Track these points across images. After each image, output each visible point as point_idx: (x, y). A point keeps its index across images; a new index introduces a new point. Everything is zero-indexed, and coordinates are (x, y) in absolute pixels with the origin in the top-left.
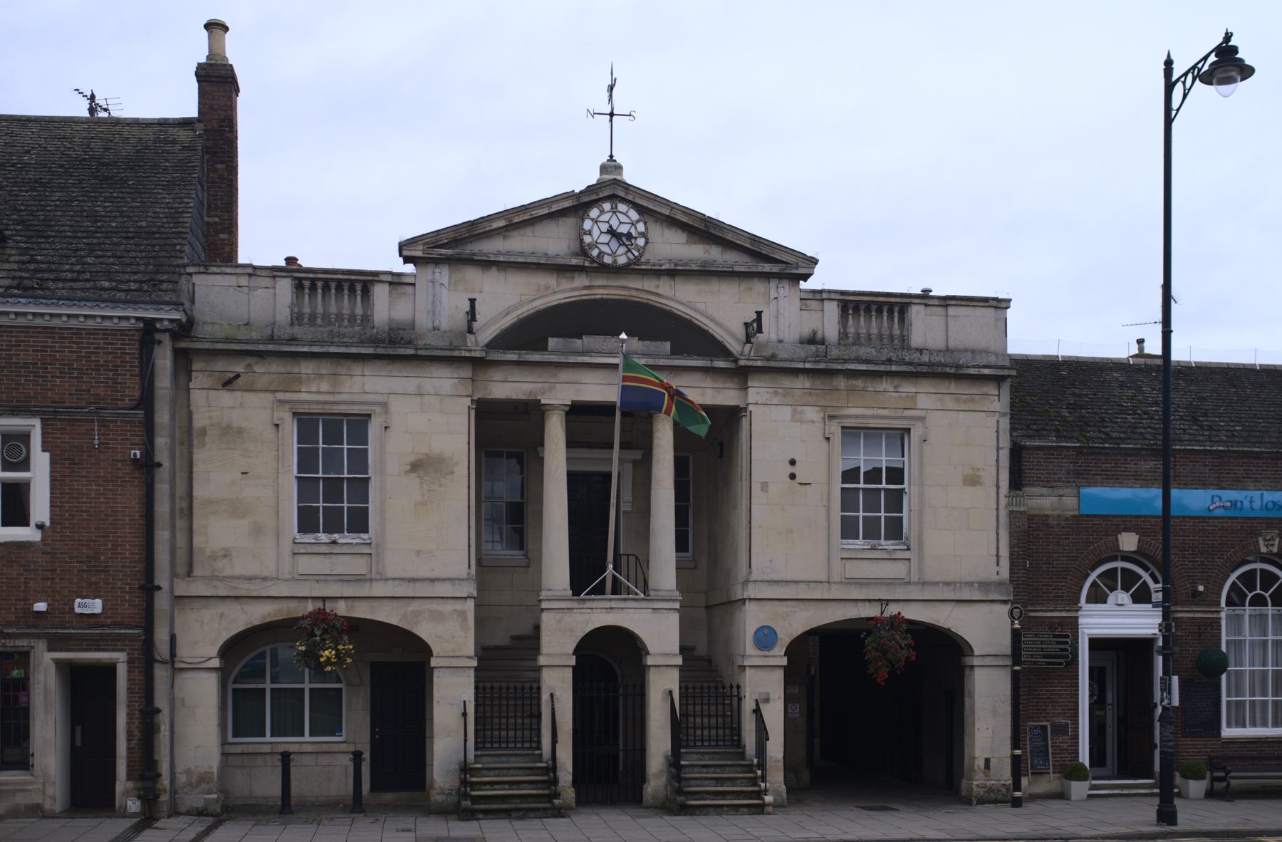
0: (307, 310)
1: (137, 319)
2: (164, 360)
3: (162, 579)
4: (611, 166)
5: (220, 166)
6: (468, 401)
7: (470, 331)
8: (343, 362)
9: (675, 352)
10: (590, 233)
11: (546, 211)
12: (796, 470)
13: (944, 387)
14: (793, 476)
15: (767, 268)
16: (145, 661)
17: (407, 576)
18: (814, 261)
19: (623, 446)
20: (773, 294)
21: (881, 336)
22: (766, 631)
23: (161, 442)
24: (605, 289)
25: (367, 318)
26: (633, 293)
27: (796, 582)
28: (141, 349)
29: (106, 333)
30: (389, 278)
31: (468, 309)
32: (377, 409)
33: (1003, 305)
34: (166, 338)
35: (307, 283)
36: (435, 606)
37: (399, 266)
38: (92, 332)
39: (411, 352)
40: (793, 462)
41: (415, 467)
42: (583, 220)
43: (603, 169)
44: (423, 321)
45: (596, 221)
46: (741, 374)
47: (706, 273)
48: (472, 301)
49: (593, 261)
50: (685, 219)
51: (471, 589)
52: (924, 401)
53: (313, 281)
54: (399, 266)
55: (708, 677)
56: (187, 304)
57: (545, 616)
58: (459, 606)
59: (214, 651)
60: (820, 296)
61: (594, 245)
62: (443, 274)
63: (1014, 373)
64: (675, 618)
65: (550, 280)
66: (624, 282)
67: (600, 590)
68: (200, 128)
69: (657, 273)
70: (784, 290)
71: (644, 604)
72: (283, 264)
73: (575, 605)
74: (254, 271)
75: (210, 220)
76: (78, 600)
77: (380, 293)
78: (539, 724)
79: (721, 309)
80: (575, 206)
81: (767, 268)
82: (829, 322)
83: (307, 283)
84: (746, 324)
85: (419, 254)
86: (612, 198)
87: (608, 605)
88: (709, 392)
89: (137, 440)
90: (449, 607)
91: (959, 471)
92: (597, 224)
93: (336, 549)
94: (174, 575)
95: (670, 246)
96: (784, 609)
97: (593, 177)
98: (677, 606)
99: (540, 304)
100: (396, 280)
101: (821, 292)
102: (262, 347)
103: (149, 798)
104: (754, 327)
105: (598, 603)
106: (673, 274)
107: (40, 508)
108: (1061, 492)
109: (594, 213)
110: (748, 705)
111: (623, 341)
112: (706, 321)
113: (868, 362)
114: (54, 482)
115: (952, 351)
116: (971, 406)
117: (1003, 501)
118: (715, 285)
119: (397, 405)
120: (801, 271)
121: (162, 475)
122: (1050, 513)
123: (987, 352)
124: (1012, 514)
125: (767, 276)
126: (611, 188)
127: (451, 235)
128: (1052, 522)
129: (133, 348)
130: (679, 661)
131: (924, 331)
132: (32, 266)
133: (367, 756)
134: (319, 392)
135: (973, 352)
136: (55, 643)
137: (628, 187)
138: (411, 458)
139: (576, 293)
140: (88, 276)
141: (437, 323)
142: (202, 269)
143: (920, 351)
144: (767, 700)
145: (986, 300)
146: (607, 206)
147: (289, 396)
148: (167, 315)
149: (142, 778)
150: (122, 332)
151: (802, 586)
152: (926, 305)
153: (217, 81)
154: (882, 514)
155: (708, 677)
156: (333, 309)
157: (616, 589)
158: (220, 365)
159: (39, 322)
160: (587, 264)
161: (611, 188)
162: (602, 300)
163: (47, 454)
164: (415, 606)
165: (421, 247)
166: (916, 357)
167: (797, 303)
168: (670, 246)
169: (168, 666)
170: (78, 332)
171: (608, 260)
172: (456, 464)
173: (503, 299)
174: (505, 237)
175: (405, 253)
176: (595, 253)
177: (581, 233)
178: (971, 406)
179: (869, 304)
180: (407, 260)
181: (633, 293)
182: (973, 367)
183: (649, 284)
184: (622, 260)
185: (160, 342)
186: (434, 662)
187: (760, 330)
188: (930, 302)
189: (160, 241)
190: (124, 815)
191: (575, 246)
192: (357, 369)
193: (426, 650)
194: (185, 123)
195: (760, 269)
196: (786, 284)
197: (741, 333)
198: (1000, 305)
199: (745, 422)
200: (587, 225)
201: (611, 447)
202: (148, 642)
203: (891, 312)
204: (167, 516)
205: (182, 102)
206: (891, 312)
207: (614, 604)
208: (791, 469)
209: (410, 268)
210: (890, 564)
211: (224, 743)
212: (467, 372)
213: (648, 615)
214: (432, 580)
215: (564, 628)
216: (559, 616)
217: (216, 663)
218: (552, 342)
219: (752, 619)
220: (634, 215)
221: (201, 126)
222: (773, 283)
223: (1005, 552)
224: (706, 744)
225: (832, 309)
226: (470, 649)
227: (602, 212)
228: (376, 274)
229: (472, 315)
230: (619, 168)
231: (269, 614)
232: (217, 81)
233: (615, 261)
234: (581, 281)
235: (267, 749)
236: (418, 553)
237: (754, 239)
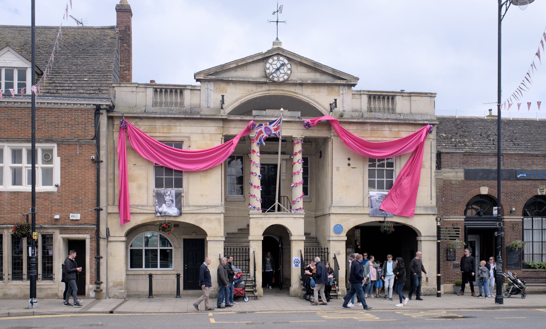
1: (93, 105)
2: (103, 120)
3: (103, 205)
4: (277, 41)
5: (125, 45)
6: (221, 136)
7: (222, 108)
8: (172, 120)
9: (303, 115)
10: (269, 69)
11: (251, 60)
15: (339, 82)
16: (97, 238)
18: (357, 79)
19: (283, 153)
20: (341, 92)
21: (384, 109)
23: (103, 152)
24: (275, 91)
25: (182, 104)
26: (286, 92)
27: (351, 207)
28: (95, 116)
29: (82, 110)
30: (190, 88)
31: (221, 99)
32: (186, 139)
33: (433, 95)
34: (104, 112)
35: (158, 90)
36: (208, 216)
37: (194, 83)
38: (77, 110)
39: (199, 116)
42: (266, 64)
43: (274, 44)
44: (204, 104)
47: (315, 84)
48: (223, 96)
50: (306, 63)
51: (222, 210)
53: (161, 89)
54: (194, 83)
55: (315, 245)
56: (113, 99)
57: (251, 220)
58: (217, 216)
59: (123, 234)
60: (360, 93)
62: (211, 86)
63: (438, 123)
64: (303, 220)
65: (253, 88)
66: (282, 88)
67: (273, 209)
68: (117, 30)
69: (295, 84)
70: (344, 91)
71: (291, 216)
72: (149, 82)
73: (262, 216)
74: (138, 86)
75: (121, 66)
76: (71, 214)
77: (187, 93)
78: (249, 263)
79: (321, 99)
80: (264, 58)
81: (339, 82)
82: (363, 103)
83: (158, 90)
84: (331, 104)
85: (202, 78)
86: (278, 54)
87: (276, 216)
89: (94, 152)
90: (214, 217)
92: (273, 64)
94: (108, 205)
96: (346, 218)
97: (270, 47)
98: (303, 216)
100: (193, 88)
101: (360, 91)
102: (141, 115)
103: (98, 291)
104: (333, 106)
105: (272, 215)
106: (301, 84)
107: (57, 179)
108: (456, 170)
109: (270, 61)
110: (331, 256)
111: (282, 112)
112: (315, 103)
113: (379, 119)
114: (62, 168)
115: (413, 114)
117: (433, 174)
118: (318, 89)
119: (194, 138)
120: (352, 83)
121: (103, 166)
122: (452, 179)
123: (427, 114)
124: (437, 179)
125: (339, 85)
126: (277, 52)
127: (214, 70)
128: (453, 182)
130: (304, 238)
132: (54, 85)
133: (182, 276)
134: (163, 133)
136: (63, 230)
137: (283, 50)
140: (75, 88)
141: (209, 105)
142: (118, 85)
143: (400, 114)
144: (339, 254)
145: (427, 94)
146: (275, 58)
148: (104, 103)
149: (96, 283)
150: (88, 110)
152: (402, 96)
153: (124, 11)
154: (385, 179)
155: (315, 245)
156: (169, 100)
157: (279, 209)
160: (268, 81)
161: (277, 52)
163: (59, 158)
164: (200, 216)
165: (203, 75)
166: (398, 117)
167: (351, 96)
168: (300, 74)
169: (106, 240)
170: (71, 110)
171: (276, 79)
173: (236, 96)
174: (235, 71)
175: (197, 78)
176: (271, 77)
177: (265, 69)
179: (379, 96)
180: (198, 80)
181: (286, 92)
182: (421, 120)
183: (292, 89)
185: (102, 114)
186: (208, 239)
187: (336, 106)
188: (404, 95)
189: (103, 74)
190: (89, 298)
191: (263, 74)
192: (178, 123)
193: (205, 234)
194: (112, 28)
195: (336, 82)
196: (346, 88)
197: (328, 107)
198: (432, 95)
199: (330, 143)
200: (268, 65)
201: (277, 153)
202: (98, 231)
203: (388, 98)
204: (105, 182)
205: (111, 20)
206: (388, 98)
207: (278, 216)
209: (199, 83)
211: (127, 270)
212: (221, 124)
213: (291, 220)
215: (259, 224)
217: (124, 239)
218: (254, 112)
219: (333, 221)
221: (118, 29)
222: (341, 88)
223: (434, 195)
225: (365, 98)
226: (222, 234)
227: (274, 60)
228: (185, 86)
229: (223, 102)
230: (280, 43)
231: (144, 220)
232: (124, 11)
235: (143, 273)
236: (202, 195)
237: (333, 70)
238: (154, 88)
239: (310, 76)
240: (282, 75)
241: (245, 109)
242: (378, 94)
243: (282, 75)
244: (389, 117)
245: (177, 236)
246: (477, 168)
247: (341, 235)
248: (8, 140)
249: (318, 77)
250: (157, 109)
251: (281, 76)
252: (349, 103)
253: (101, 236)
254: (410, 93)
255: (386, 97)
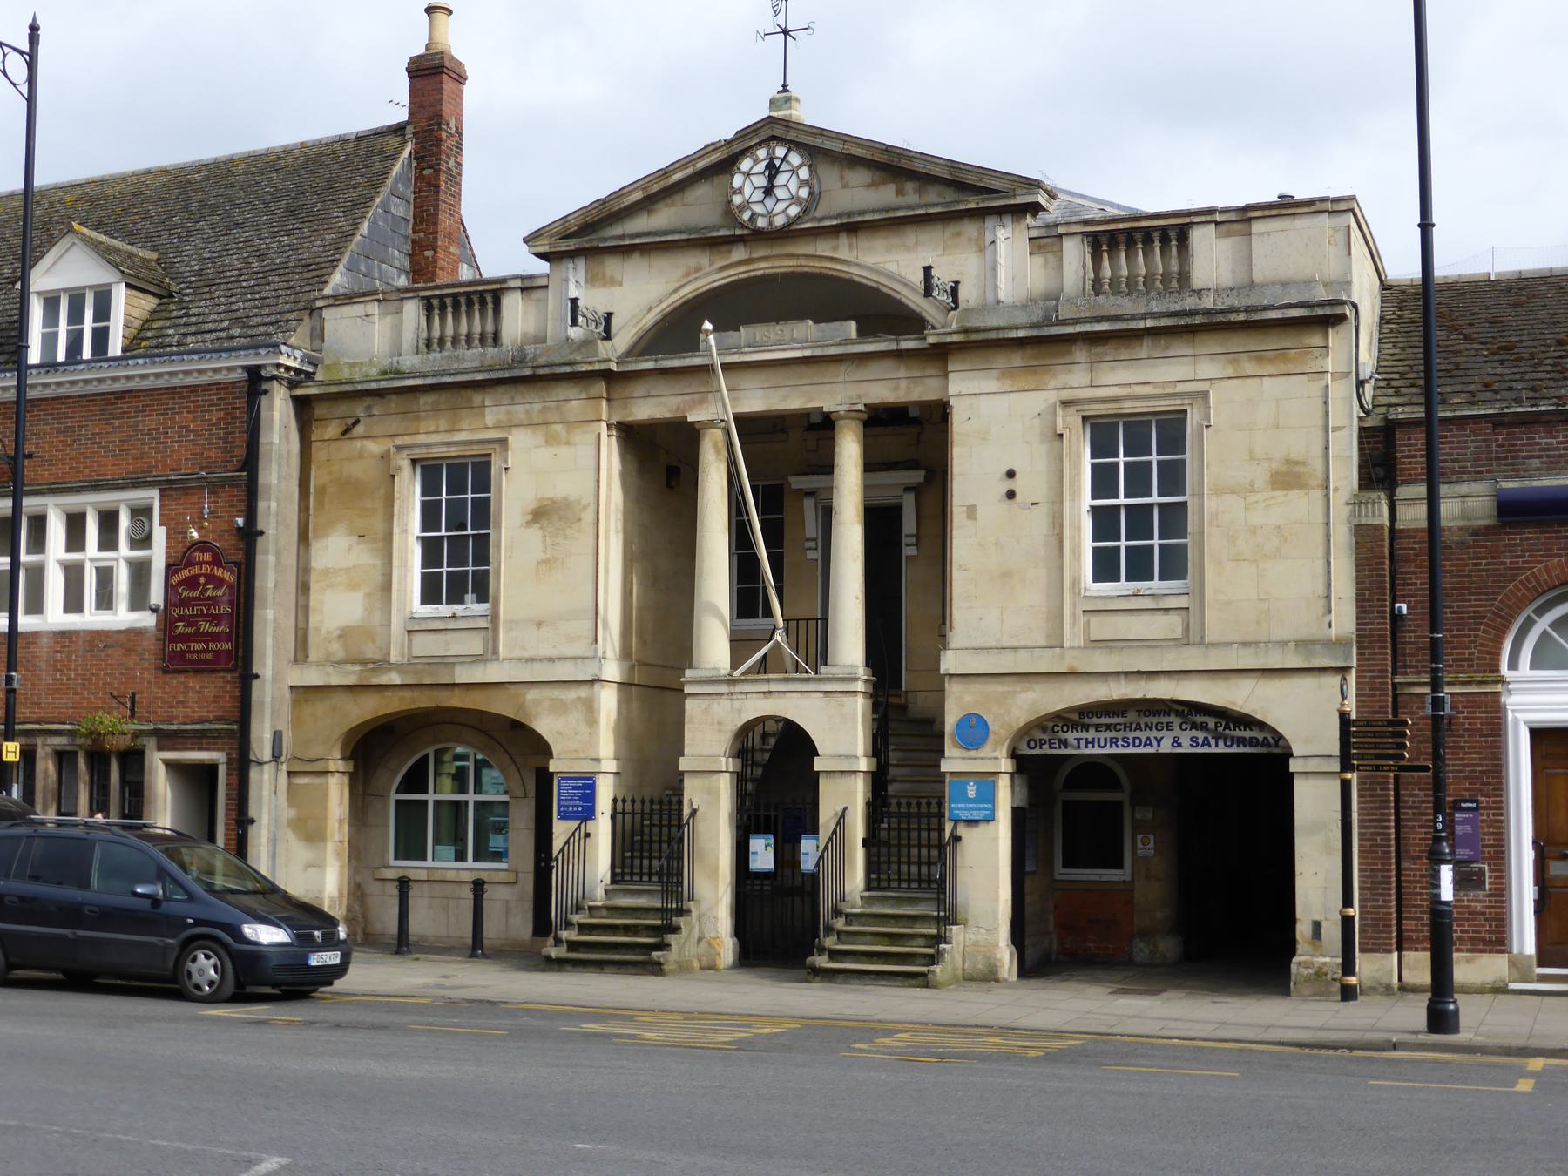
0: (436, 334)
2: (278, 409)
8: (463, 392)
9: (863, 333)
10: (740, 191)
11: (689, 171)
12: (1017, 484)
13: (1238, 342)
14: (1011, 495)
16: (242, 763)
17: (527, 655)
20: (989, 237)
22: (974, 721)
27: (1015, 648)
30: (518, 283)
32: (497, 446)
36: (556, 693)
39: (527, 372)
40: (1011, 474)
41: (541, 514)
42: (732, 176)
45: (748, 175)
46: (940, 354)
49: (743, 226)
52: (1208, 369)
57: (689, 704)
61: (746, 205)
65: (701, 259)
69: (834, 231)
83: (435, 302)
86: (773, 138)
87: (765, 688)
88: (903, 384)
90: (572, 694)
91: (1278, 467)
93: (452, 624)
95: (856, 194)
99: (688, 291)
100: (527, 284)
102: (374, 386)
108: (1464, 489)
116: (1283, 368)
119: (519, 440)
123: (1309, 283)
125: (979, 214)
129: (241, 403)
131: (1212, 263)
134: (437, 432)
135: (1285, 284)
138: (533, 506)
139: (732, 272)
147: (407, 440)
151: (1023, 654)
153: (432, 75)
154: (1156, 542)
158: (342, 409)
159: (161, 383)
162: (763, 276)
166: (1190, 303)
168: (856, 194)
171: (761, 223)
172: (585, 508)
173: (637, 296)
174: (650, 212)
176: (746, 216)
178: (1283, 368)
179: (1130, 233)
180: (542, 256)
181: (803, 262)
183: (823, 248)
184: (779, 221)
194: (398, 129)
196: (1007, 220)
200: (737, 181)
203: (1165, 240)
207: (774, 687)
208: (1009, 485)
209: (543, 267)
210: (1161, 619)
213: (818, 700)
214: (551, 660)
216: (704, 703)
220: (795, 159)
222: (990, 222)
224: (636, 878)
225: (1074, 253)
228: (503, 280)
232: (432, 75)
233: (771, 223)
234: (739, 253)
237: (952, 165)
238: (423, 298)
239: (885, 196)
240: (781, 206)
241: (675, 330)
242: (1121, 226)
243: (781, 206)
244: (1156, 307)
245: (518, 760)
246: (1527, 483)
247: (981, 753)
248: (53, 491)
249: (912, 199)
250: (436, 359)
251: (782, 211)
252: (1003, 271)
253: (252, 757)
254: (1246, 209)
255: (1156, 236)
